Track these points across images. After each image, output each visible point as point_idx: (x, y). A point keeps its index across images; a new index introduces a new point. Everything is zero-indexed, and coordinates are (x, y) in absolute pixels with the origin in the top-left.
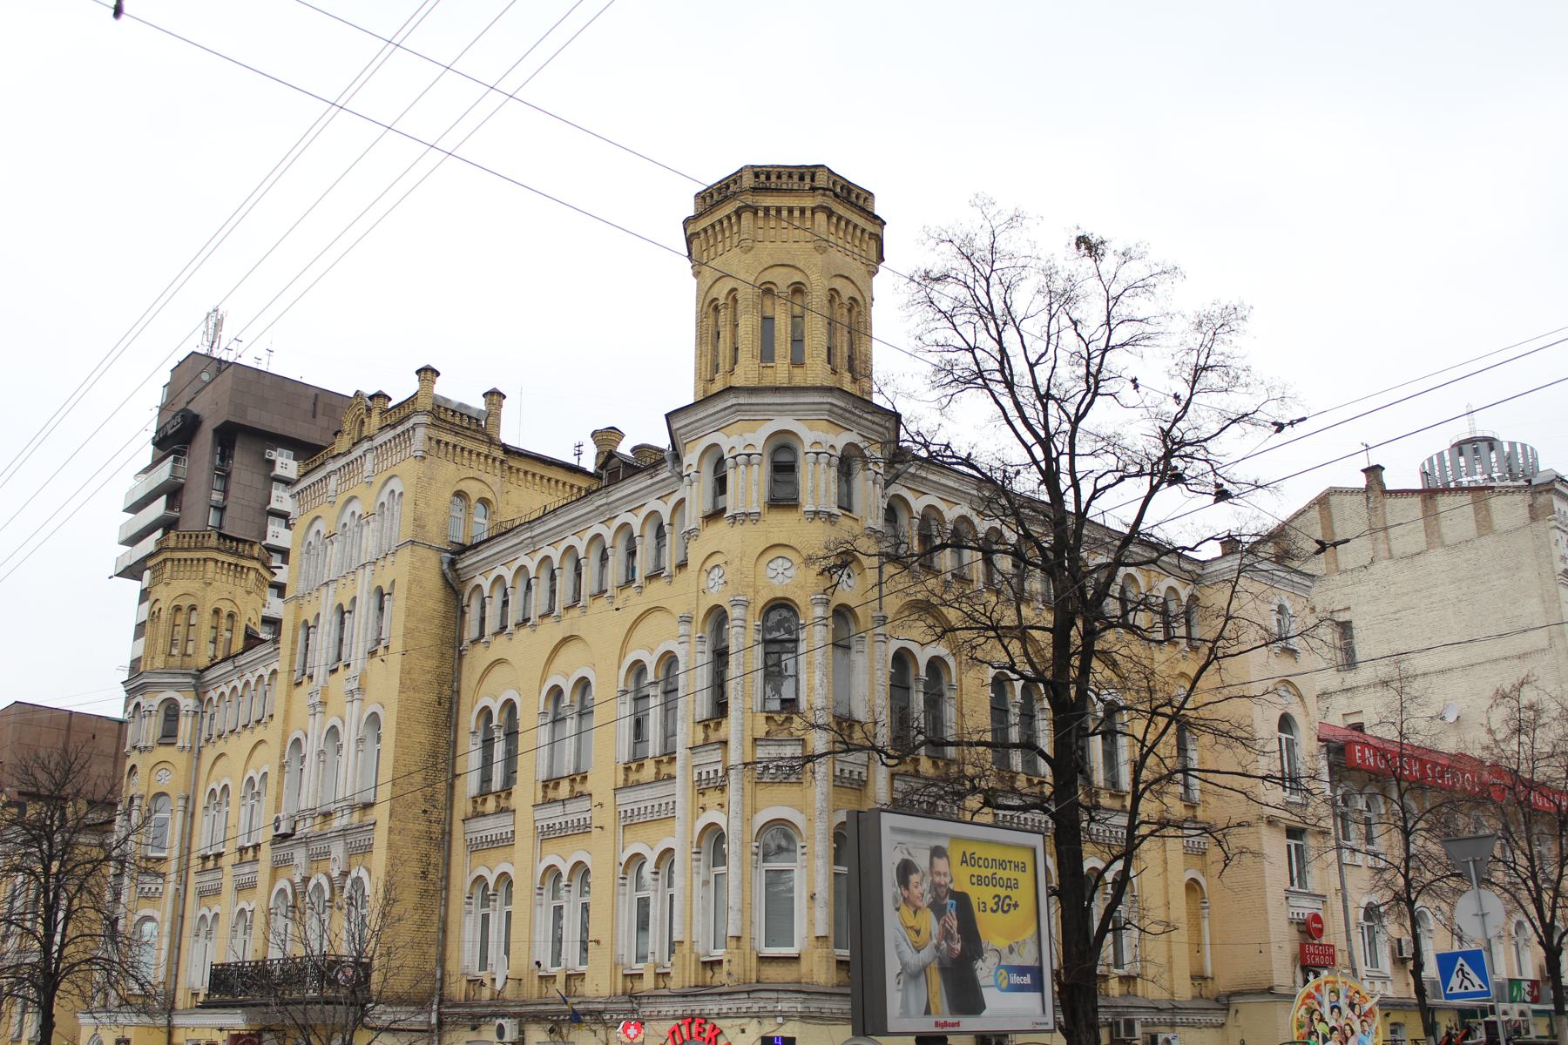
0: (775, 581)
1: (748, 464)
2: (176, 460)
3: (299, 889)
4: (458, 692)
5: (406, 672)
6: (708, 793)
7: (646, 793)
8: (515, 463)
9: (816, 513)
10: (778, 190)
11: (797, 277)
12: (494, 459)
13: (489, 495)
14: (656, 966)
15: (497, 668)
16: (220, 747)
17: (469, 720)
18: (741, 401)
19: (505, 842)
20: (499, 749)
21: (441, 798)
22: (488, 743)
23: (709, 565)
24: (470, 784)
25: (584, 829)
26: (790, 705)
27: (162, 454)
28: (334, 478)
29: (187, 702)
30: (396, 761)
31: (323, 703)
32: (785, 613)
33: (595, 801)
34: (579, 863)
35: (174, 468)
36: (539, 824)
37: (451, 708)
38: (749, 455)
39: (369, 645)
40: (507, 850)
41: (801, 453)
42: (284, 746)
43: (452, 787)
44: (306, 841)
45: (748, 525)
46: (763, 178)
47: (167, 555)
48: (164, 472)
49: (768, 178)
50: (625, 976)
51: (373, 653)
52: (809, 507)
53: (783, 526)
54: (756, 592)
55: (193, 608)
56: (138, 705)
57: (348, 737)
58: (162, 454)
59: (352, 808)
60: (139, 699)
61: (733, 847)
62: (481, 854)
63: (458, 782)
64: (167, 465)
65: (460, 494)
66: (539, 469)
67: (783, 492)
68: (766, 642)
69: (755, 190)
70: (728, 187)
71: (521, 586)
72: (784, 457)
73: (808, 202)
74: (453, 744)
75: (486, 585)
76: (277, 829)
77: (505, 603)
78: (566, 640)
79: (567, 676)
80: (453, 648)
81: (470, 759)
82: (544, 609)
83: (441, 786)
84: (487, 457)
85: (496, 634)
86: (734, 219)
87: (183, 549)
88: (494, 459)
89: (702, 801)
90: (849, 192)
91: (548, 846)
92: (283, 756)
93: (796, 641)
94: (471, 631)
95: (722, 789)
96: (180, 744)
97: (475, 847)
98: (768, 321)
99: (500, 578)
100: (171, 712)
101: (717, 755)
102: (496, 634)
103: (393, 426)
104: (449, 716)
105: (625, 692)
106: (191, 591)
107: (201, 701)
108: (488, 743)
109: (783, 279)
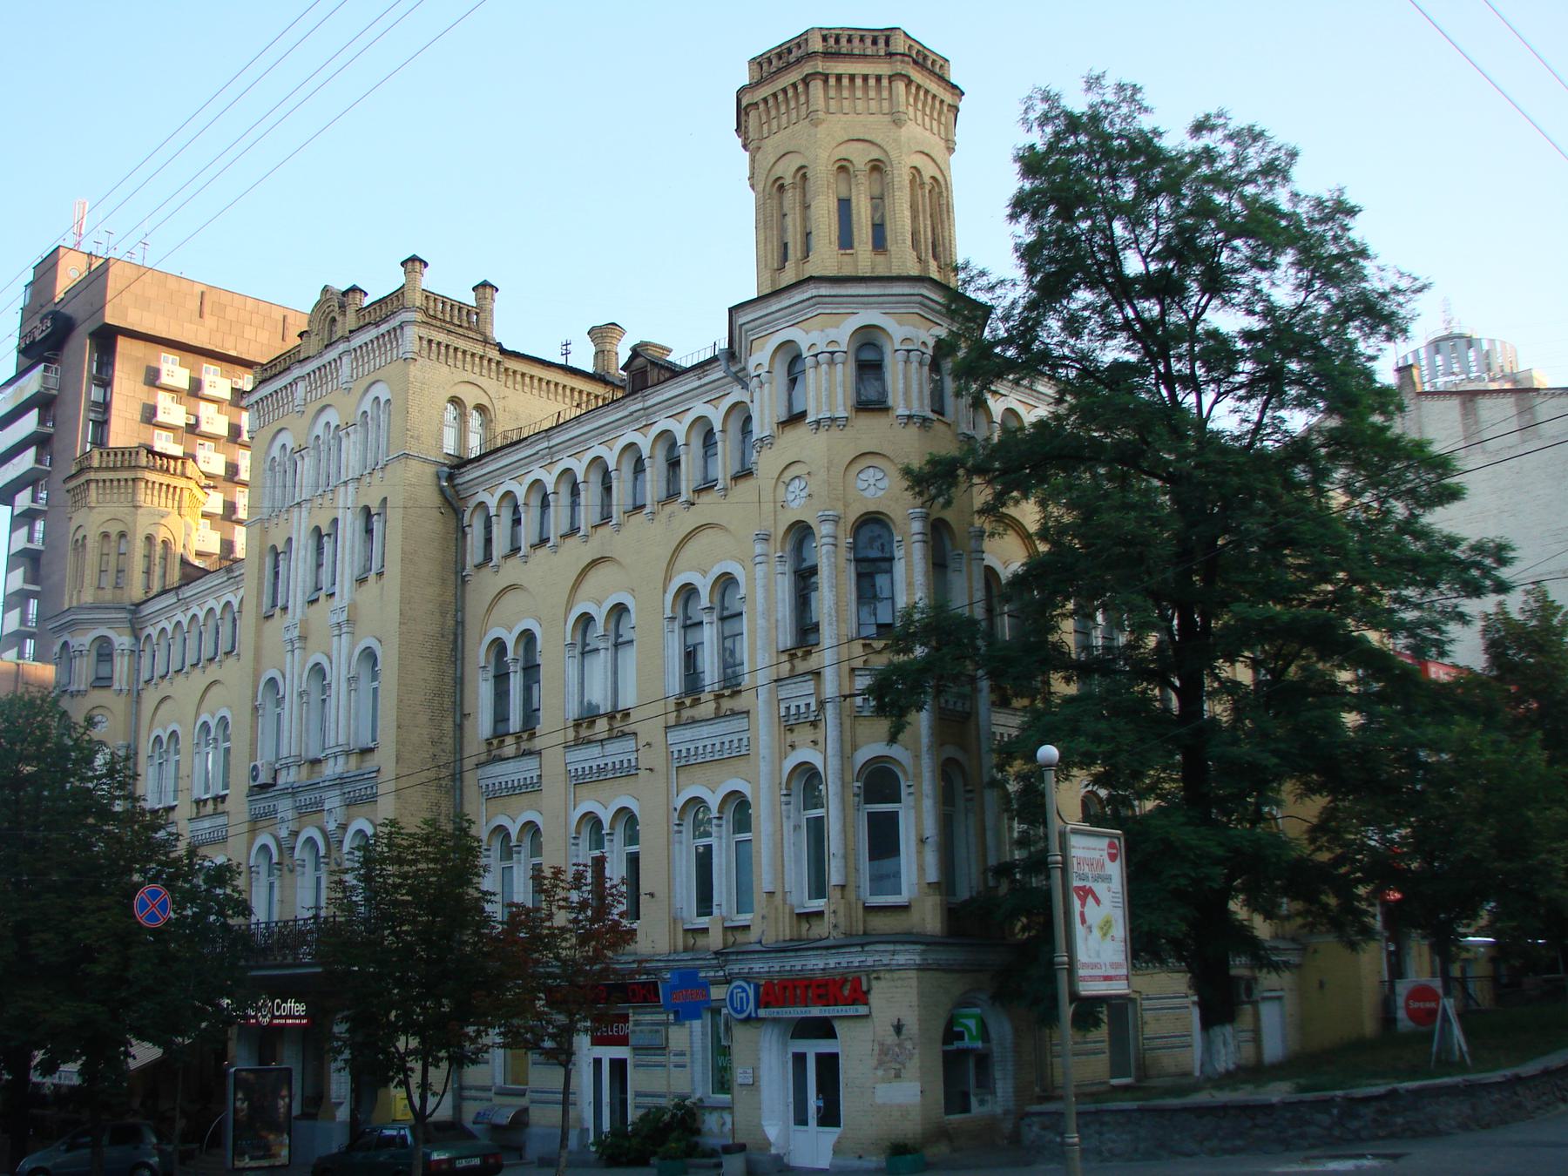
0: (866, 494)
1: (832, 363)
2: (46, 369)
3: (285, 845)
4: (463, 623)
5: (405, 601)
6: (797, 729)
7: (706, 730)
8: (513, 365)
9: (910, 417)
10: (850, 55)
11: (876, 154)
12: (490, 360)
13: (485, 401)
14: (724, 919)
15: (509, 596)
16: (165, 688)
17: (478, 653)
18: (823, 291)
19: (532, 788)
20: (516, 682)
21: (448, 740)
22: (501, 678)
23: (787, 476)
24: (482, 724)
25: (628, 772)
27: (28, 362)
28: (301, 385)
29: (122, 641)
30: (400, 701)
31: (303, 638)
32: (877, 529)
33: (641, 742)
34: (623, 810)
35: (45, 378)
36: (571, 768)
37: (455, 641)
38: (832, 353)
39: (356, 573)
40: (533, 796)
41: (888, 350)
42: (256, 687)
43: (459, 727)
44: (293, 791)
45: (835, 432)
46: (832, 41)
47: (92, 476)
48: (33, 383)
49: (837, 41)
50: (686, 931)
51: (361, 581)
52: (901, 411)
53: (871, 432)
54: (846, 505)
55: (122, 535)
56: (66, 644)
57: (338, 675)
58: (28, 362)
59: (348, 753)
60: (66, 637)
61: (831, 789)
62: (500, 801)
63: (467, 723)
64: (37, 373)
65: (455, 401)
66: (538, 371)
67: (871, 393)
68: (858, 561)
69: (827, 55)
70: (790, 51)
71: (535, 501)
72: (868, 355)
73: (884, 69)
74: (459, 682)
75: (492, 502)
76: (255, 778)
77: (517, 522)
78: (594, 563)
79: (599, 603)
80: (458, 577)
81: (482, 693)
82: (565, 527)
83: (448, 725)
84: (482, 358)
85: (506, 557)
86: (800, 88)
87: (108, 469)
88: (490, 360)
89: (790, 738)
90: (925, 58)
91: (583, 791)
92: (255, 697)
93: (891, 559)
94: (474, 554)
95: (814, 724)
96: (116, 686)
97: (492, 795)
98: (845, 205)
99: (508, 494)
100: (104, 651)
101: (809, 687)
102: (506, 557)
103: (377, 325)
104: (455, 649)
105: (672, 619)
106: (119, 516)
107: (137, 638)
108: (501, 678)
109: (860, 157)
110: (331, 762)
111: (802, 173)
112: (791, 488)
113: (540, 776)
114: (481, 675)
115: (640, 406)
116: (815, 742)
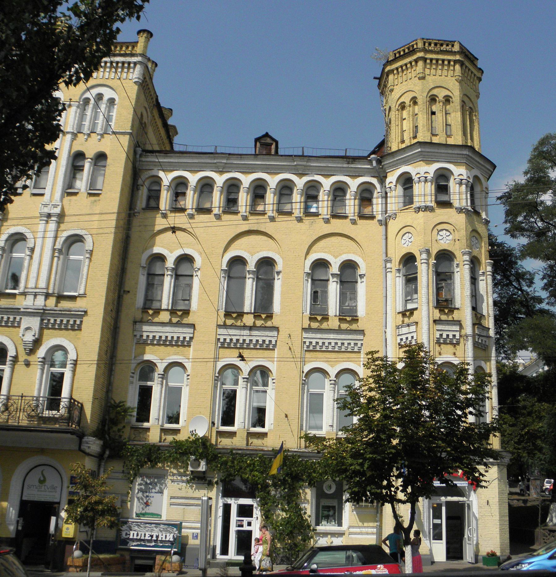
19: (185, 344)
95: (455, 345)
110: (30, 298)
112: (441, 233)
113: (191, 338)
114: (141, 271)
115: (304, 163)
116: (455, 354)
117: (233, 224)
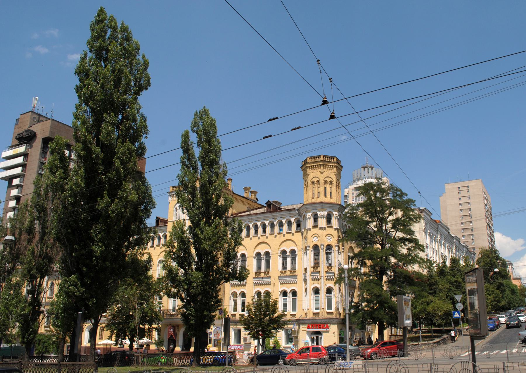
11: (331, 180)
23: (314, 236)
26: (330, 265)
53: (330, 231)
66: (238, 197)
95: (319, 280)
98: (325, 188)
109: (329, 180)
111: (318, 181)
117: (256, 241)
